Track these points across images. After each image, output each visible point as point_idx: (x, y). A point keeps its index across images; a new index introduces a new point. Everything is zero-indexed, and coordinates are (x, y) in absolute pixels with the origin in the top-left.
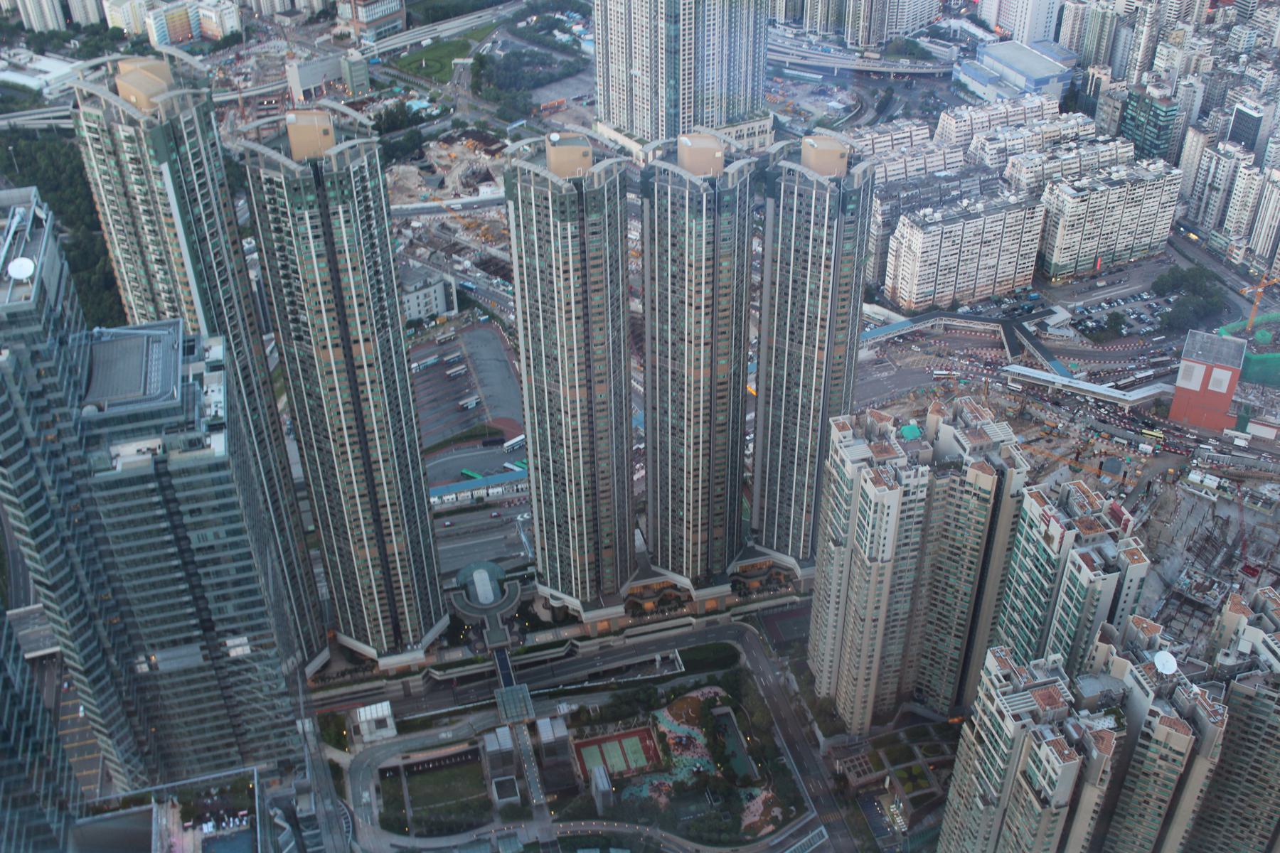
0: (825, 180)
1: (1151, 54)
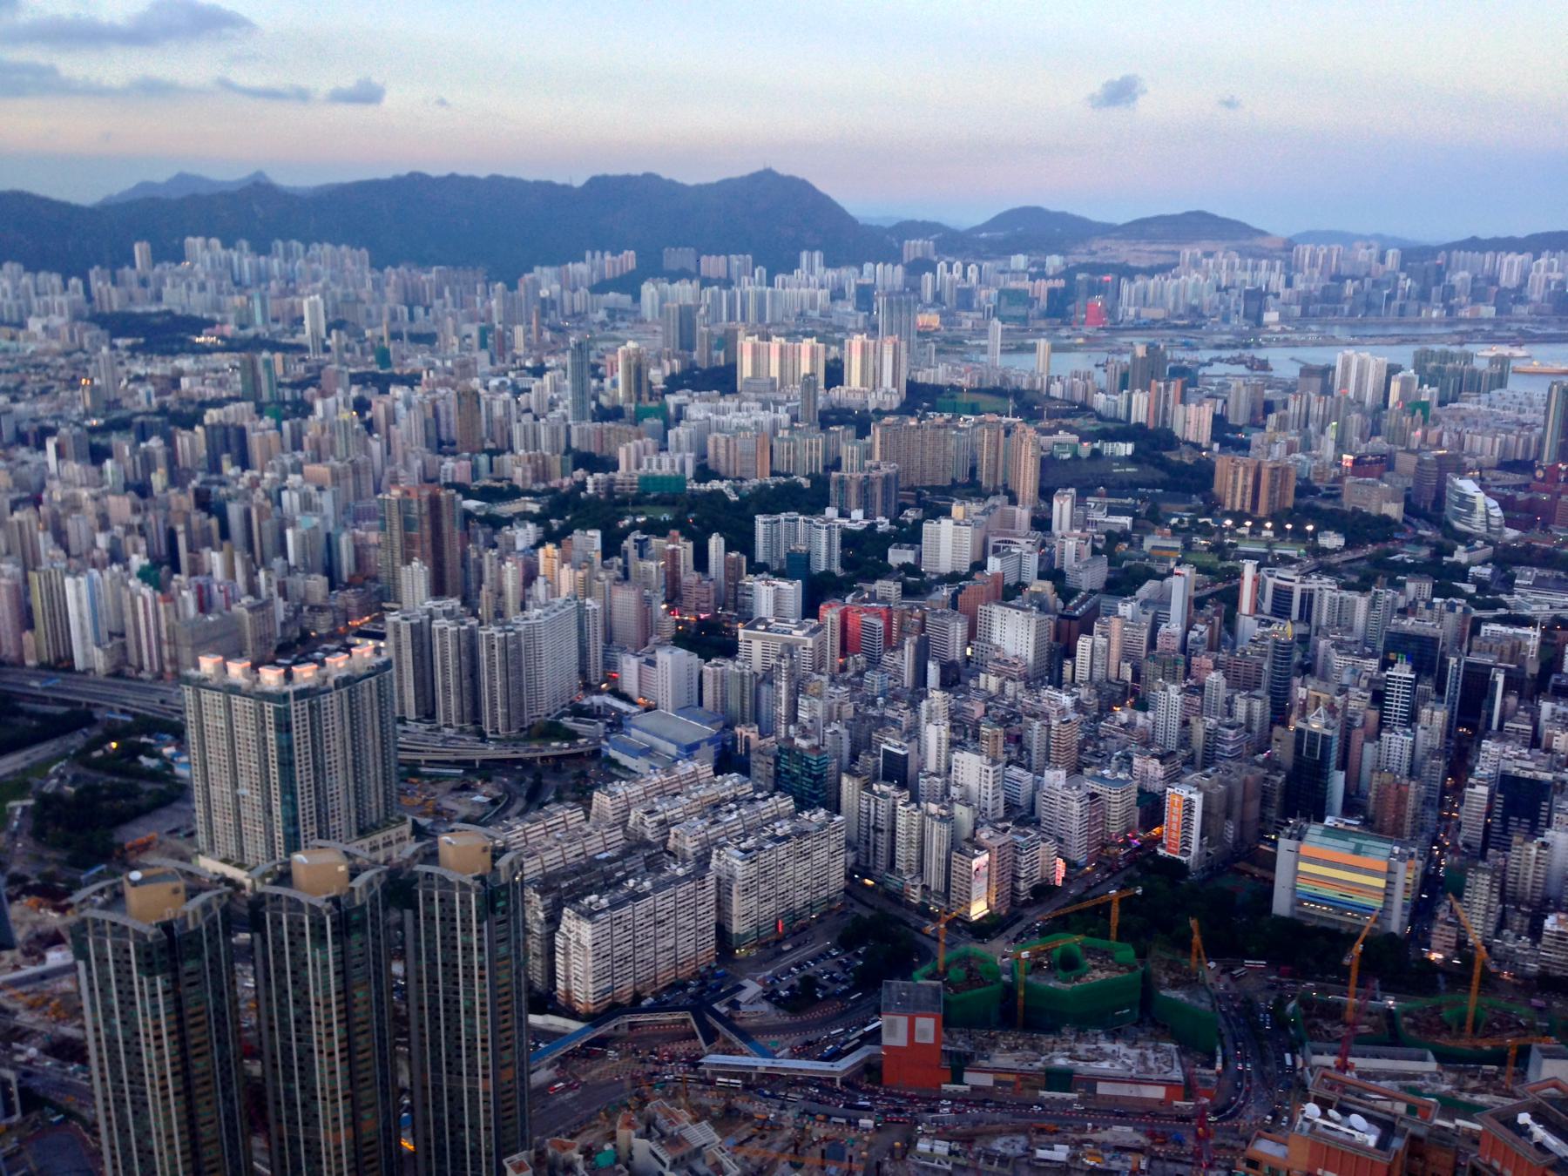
0: (468, 879)
1: (794, 707)
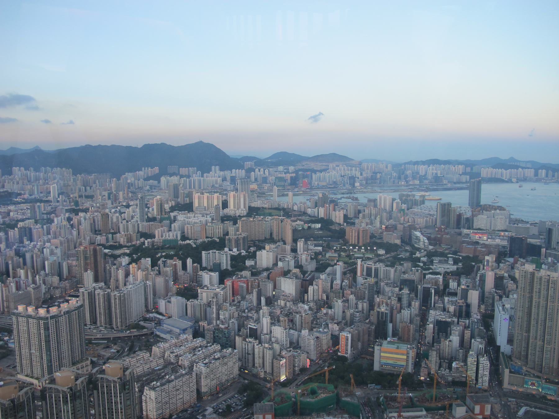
0: (116, 379)
1: (218, 314)
